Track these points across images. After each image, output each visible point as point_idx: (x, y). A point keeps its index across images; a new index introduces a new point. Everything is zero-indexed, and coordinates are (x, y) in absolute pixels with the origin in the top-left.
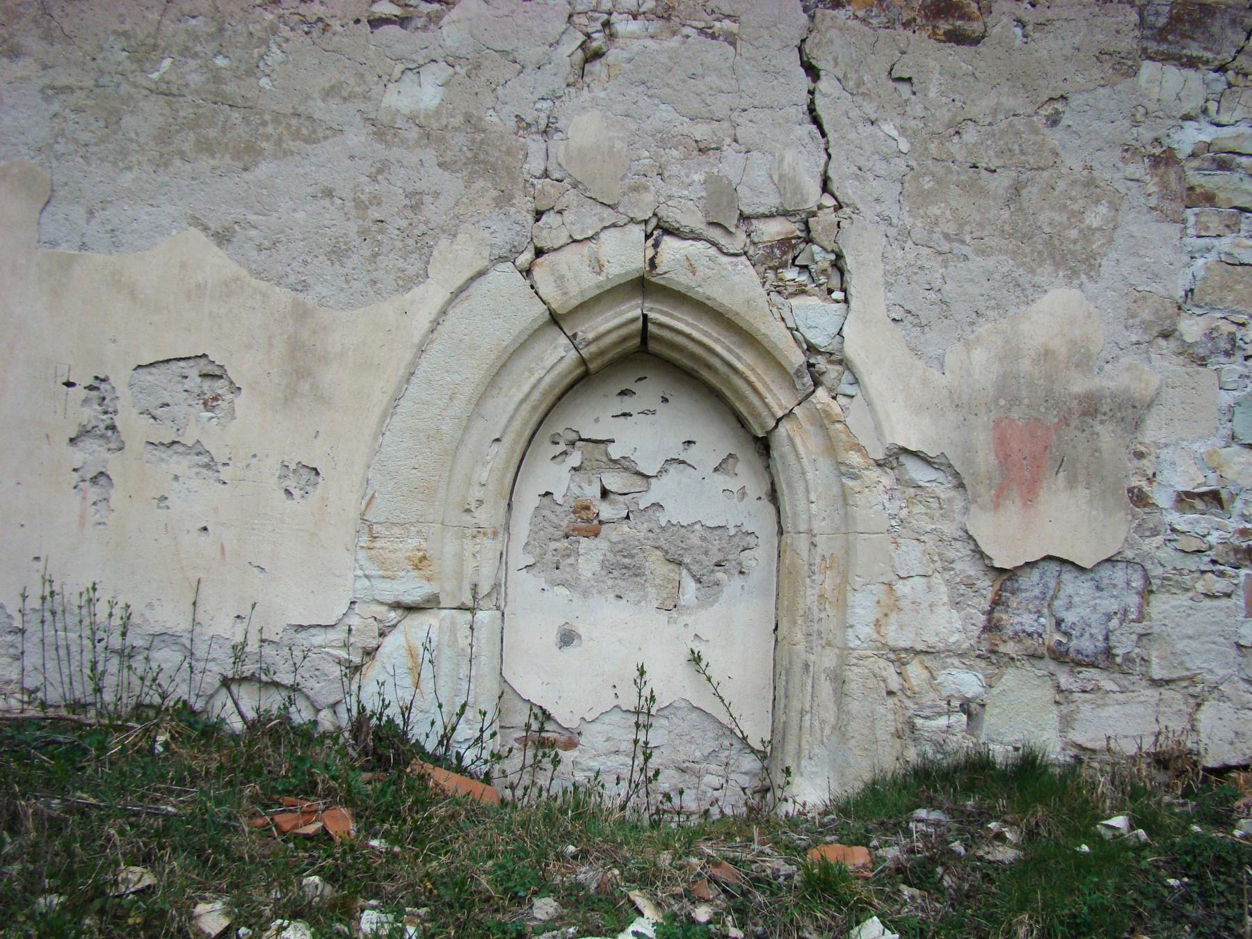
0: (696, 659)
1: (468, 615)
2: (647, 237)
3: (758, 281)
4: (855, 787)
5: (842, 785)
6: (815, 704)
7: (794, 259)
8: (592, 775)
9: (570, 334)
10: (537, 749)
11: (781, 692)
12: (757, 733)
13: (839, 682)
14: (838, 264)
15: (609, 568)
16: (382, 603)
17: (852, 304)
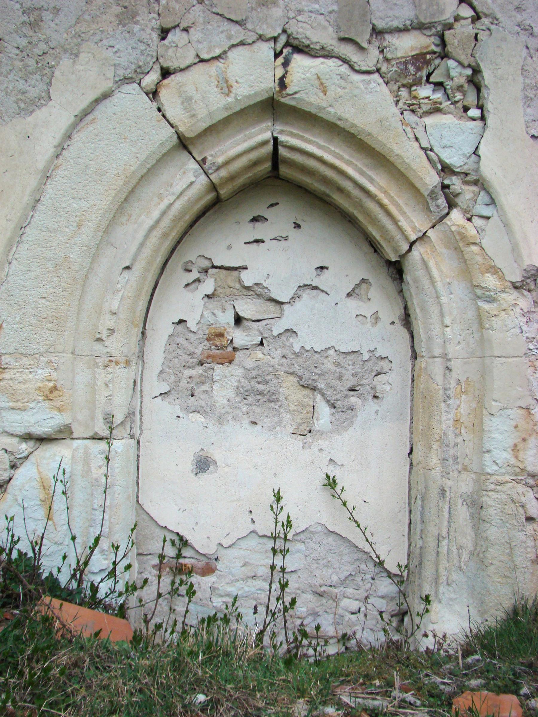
0: (331, 483)
1: (103, 445)
2: (277, 55)
3: (391, 99)
4: (494, 617)
5: (482, 613)
6: (452, 530)
7: (429, 75)
8: (230, 600)
9: (199, 159)
10: (175, 575)
11: (417, 517)
12: (394, 558)
13: (477, 507)
14: (475, 81)
15: (243, 395)
16: (12, 435)
17: (491, 120)
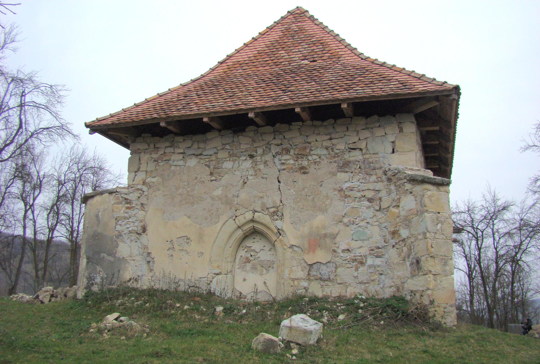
0: (265, 283)
15: (252, 268)
